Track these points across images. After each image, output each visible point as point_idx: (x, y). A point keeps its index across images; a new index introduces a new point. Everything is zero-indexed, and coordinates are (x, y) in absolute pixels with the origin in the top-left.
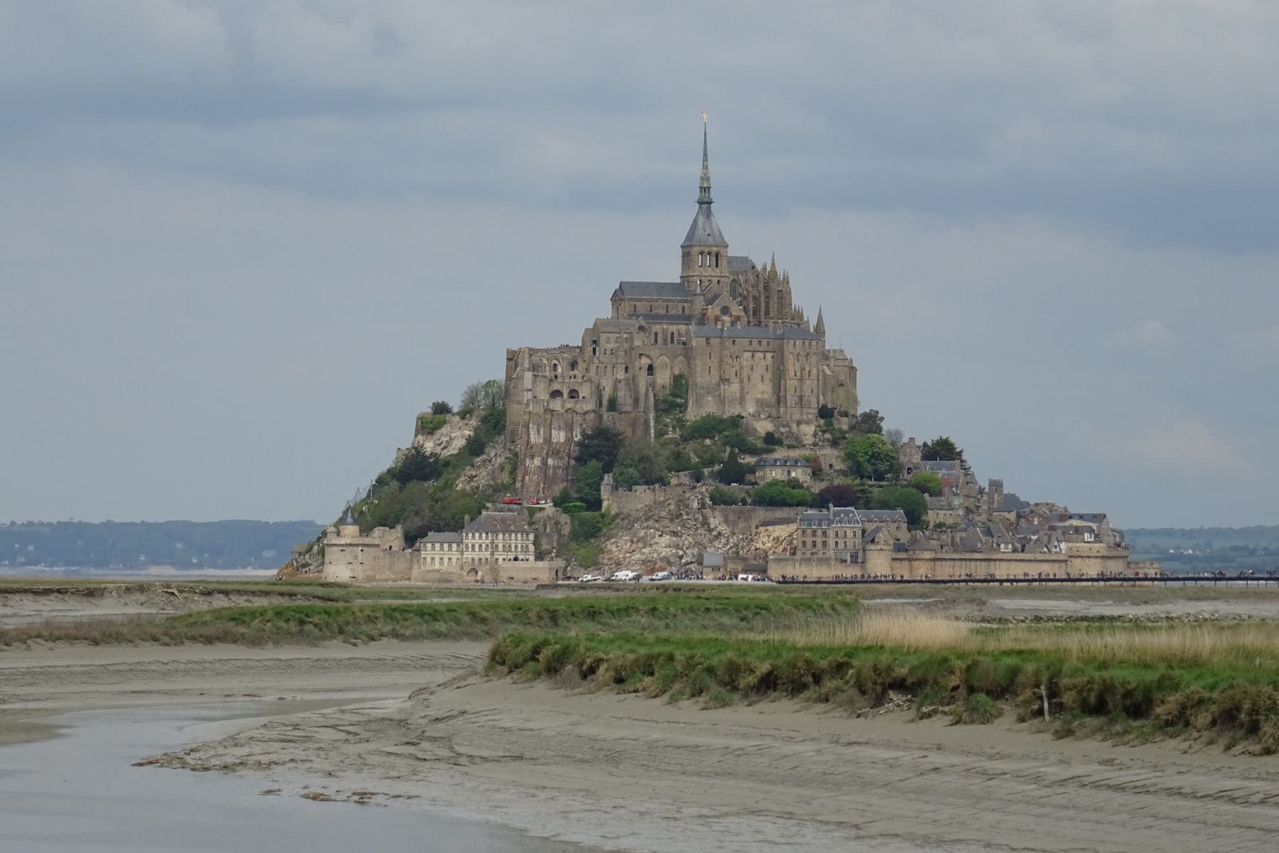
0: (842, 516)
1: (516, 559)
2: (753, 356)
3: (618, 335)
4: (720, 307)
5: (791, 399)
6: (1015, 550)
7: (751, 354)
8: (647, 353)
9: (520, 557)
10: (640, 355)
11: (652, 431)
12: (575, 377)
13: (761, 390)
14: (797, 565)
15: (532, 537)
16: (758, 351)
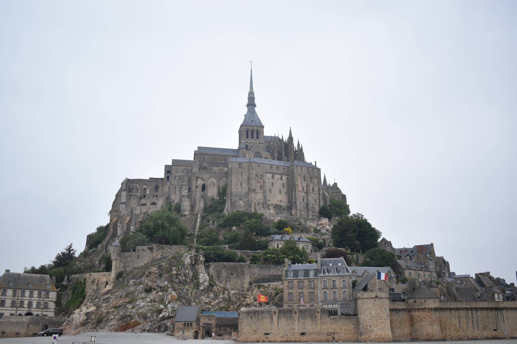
0: (331, 265)
1: (29, 314)
2: (273, 177)
3: (184, 168)
4: (254, 152)
5: (300, 204)
6: (504, 300)
7: (271, 175)
8: (199, 176)
9: (35, 313)
10: (197, 177)
11: (198, 224)
12: (157, 196)
13: (279, 200)
14: (275, 318)
15: (53, 295)
16: (276, 174)
